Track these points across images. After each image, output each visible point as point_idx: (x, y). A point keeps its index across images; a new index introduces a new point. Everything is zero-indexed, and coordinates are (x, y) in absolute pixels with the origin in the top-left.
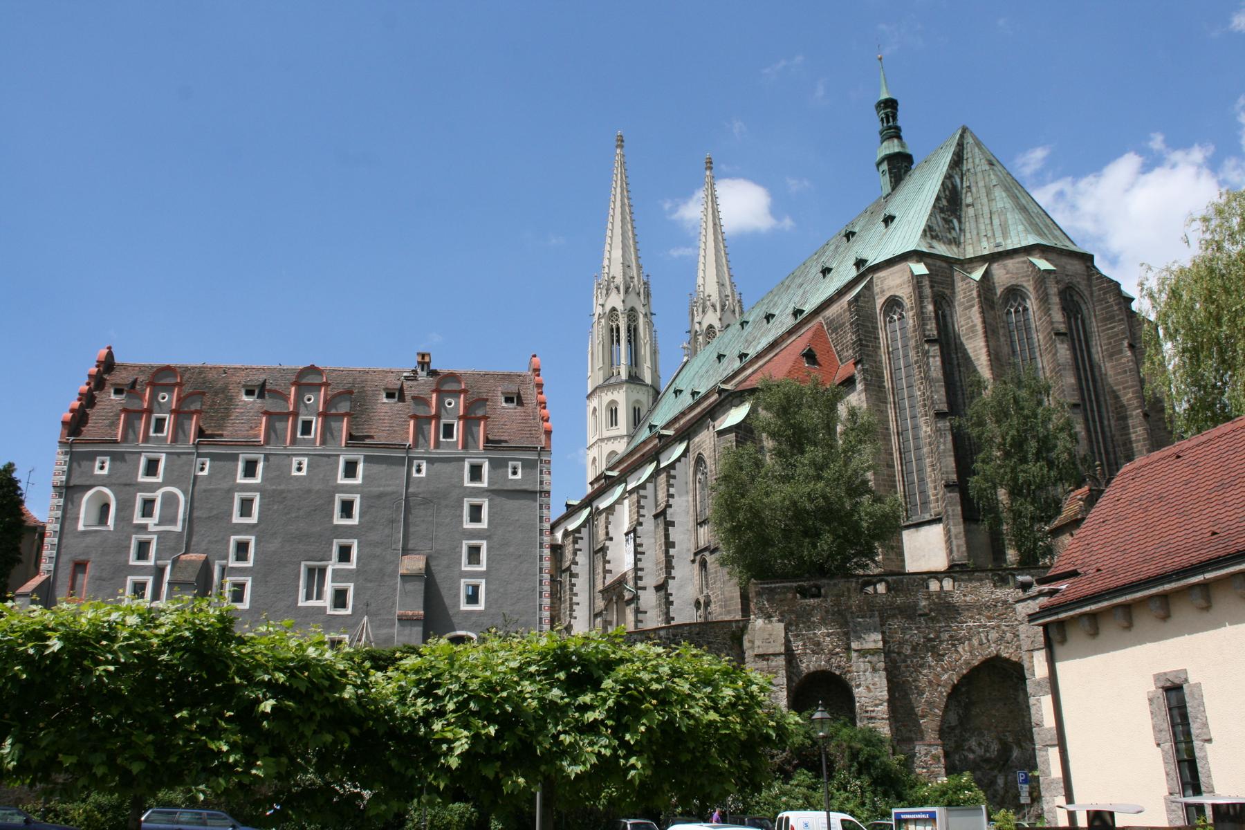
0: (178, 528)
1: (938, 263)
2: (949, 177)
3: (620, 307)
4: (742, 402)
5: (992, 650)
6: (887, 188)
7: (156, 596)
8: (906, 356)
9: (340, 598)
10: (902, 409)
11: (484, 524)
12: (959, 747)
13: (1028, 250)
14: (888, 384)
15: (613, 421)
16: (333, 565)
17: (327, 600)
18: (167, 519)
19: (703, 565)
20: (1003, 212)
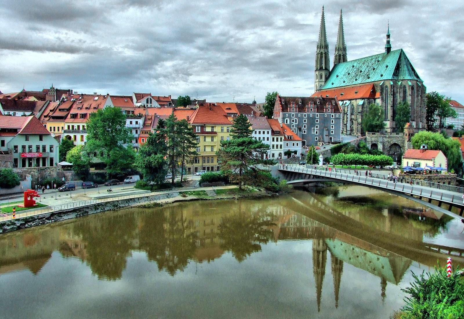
0: (297, 124)
1: (394, 80)
2: (398, 62)
3: (323, 52)
4: (362, 100)
5: (395, 142)
6: (386, 54)
7: (295, 132)
8: (387, 95)
9: (317, 133)
10: (386, 103)
11: (333, 123)
12: (389, 152)
13: (408, 80)
14: (384, 99)
15: (321, 77)
16: (316, 128)
17: (315, 133)
18: (296, 122)
19: (352, 121)
20: (405, 71)
